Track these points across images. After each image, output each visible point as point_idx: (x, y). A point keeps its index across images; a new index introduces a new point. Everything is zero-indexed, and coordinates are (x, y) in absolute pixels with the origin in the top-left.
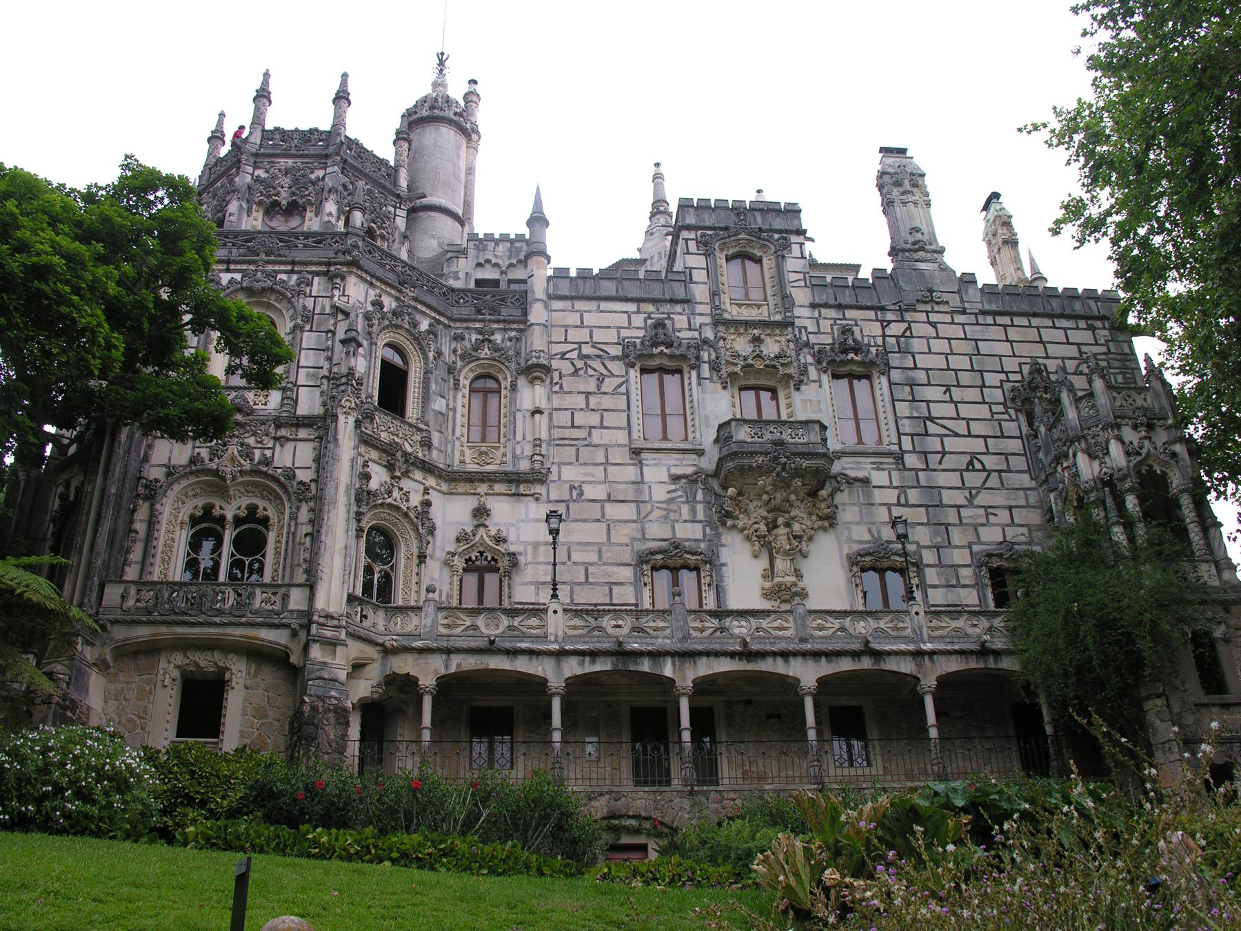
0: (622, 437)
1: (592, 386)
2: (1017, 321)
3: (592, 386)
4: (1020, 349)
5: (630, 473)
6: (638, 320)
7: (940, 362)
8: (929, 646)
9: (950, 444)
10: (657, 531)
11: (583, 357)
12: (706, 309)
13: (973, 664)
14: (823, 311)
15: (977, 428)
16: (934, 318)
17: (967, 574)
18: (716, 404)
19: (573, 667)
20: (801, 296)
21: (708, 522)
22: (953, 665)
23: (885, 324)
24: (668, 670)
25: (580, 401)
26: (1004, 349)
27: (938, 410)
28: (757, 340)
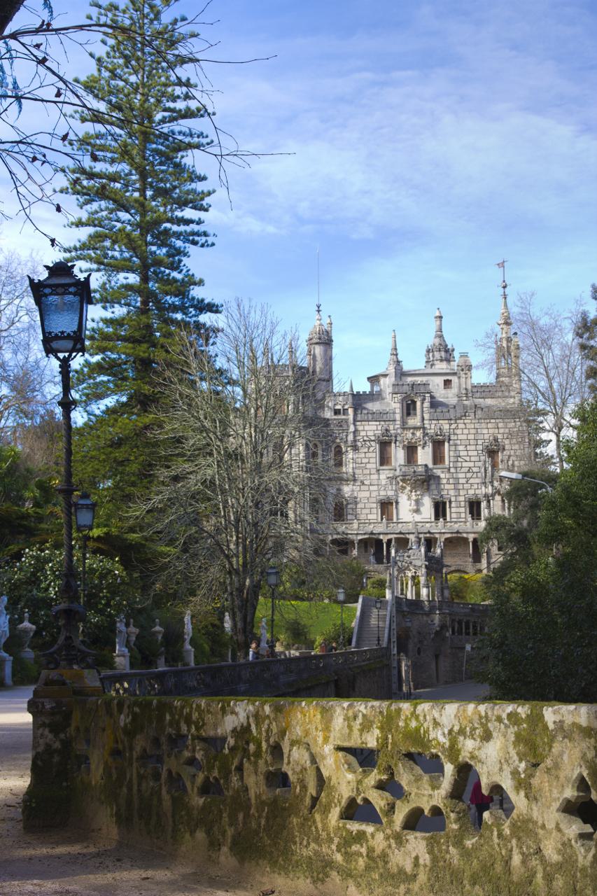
0: (374, 466)
1: (366, 450)
2: (492, 421)
3: (366, 450)
4: (491, 431)
5: (375, 477)
6: (379, 428)
7: (465, 437)
8: (443, 531)
9: (465, 464)
10: (382, 493)
11: (364, 441)
12: (398, 422)
13: (454, 535)
14: (433, 422)
15: (473, 459)
16: (466, 421)
17: (463, 504)
18: (398, 455)
19: (360, 537)
20: (426, 416)
21: (396, 491)
22: (449, 536)
23: (450, 424)
24: (381, 537)
25: (363, 455)
26: (485, 431)
27: (462, 453)
28: (413, 434)
